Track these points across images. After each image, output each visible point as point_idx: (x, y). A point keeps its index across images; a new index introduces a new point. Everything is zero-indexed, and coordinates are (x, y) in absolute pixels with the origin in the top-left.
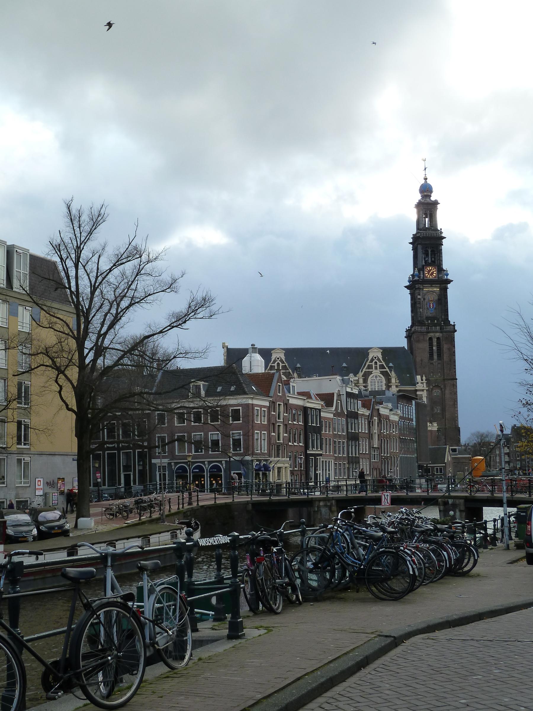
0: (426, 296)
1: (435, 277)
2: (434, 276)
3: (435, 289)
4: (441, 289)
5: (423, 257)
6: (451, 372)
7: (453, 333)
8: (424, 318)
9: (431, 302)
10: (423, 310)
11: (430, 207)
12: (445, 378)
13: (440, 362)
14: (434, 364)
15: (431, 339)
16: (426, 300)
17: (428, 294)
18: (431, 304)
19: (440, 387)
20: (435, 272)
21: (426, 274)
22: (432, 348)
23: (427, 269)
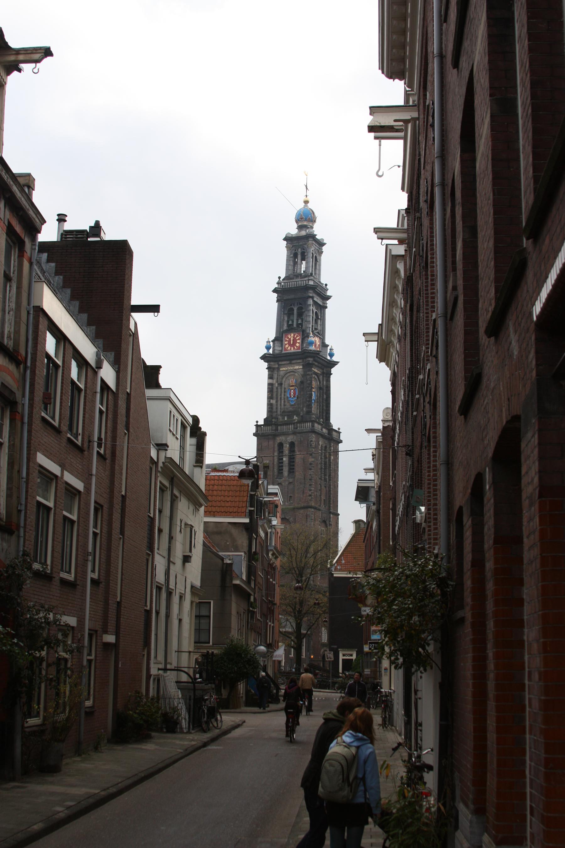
0: (284, 379)
1: (298, 348)
2: (297, 346)
3: (297, 367)
4: (303, 365)
5: (284, 319)
6: (305, 495)
7: (310, 434)
8: (279, 413)
10: (277, 402)
11: (301, 243)
12: (296, 505)
13: (291, 480)
14: (283, 484)
15: (281, 445)
16: (285, 385)
17: (287, 376)
18: (292, 391)
19: (288, 520)
20: (298, 341)
21: (286, 344)
22: (282, 459)
23: (288, 338)
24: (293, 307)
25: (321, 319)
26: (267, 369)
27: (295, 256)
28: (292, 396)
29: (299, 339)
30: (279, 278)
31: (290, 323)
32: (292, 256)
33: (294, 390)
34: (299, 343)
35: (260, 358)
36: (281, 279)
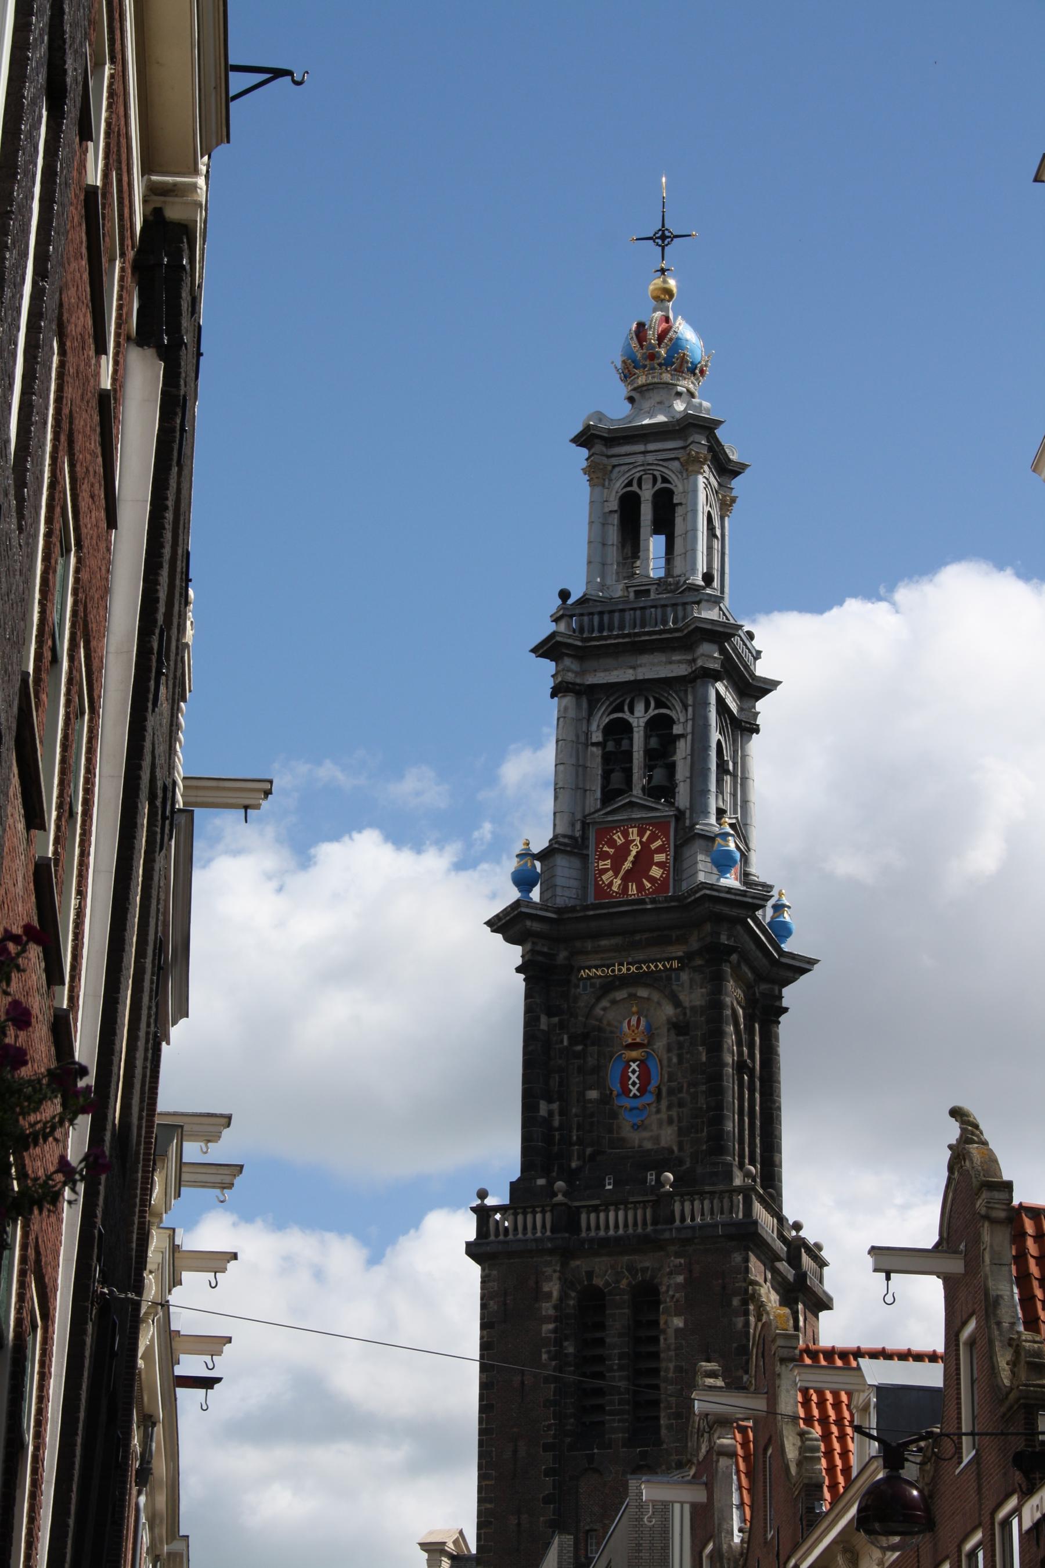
2: (652, 880)
9: (634, 1054)
18: (634, 1066)
20: (659, 858)
23: (612, 843)
24: (626, 715)
25: (734, 776)
26: (519, 970)
27: (629, 504)
28: (634, 1090)
29: (660, 849)
30: (564, 595)
31: (617, 777)
32: (614, 505)
33: (643, 1064)
34: (660, 865)
35: (489, 923)
36: (570, 602)
